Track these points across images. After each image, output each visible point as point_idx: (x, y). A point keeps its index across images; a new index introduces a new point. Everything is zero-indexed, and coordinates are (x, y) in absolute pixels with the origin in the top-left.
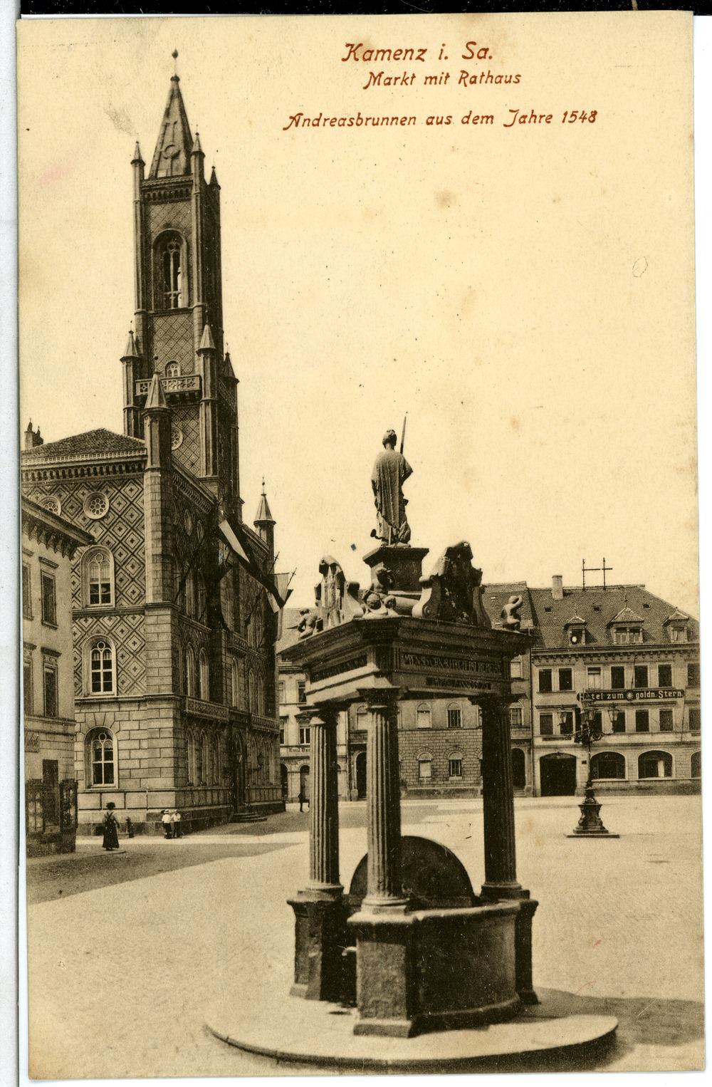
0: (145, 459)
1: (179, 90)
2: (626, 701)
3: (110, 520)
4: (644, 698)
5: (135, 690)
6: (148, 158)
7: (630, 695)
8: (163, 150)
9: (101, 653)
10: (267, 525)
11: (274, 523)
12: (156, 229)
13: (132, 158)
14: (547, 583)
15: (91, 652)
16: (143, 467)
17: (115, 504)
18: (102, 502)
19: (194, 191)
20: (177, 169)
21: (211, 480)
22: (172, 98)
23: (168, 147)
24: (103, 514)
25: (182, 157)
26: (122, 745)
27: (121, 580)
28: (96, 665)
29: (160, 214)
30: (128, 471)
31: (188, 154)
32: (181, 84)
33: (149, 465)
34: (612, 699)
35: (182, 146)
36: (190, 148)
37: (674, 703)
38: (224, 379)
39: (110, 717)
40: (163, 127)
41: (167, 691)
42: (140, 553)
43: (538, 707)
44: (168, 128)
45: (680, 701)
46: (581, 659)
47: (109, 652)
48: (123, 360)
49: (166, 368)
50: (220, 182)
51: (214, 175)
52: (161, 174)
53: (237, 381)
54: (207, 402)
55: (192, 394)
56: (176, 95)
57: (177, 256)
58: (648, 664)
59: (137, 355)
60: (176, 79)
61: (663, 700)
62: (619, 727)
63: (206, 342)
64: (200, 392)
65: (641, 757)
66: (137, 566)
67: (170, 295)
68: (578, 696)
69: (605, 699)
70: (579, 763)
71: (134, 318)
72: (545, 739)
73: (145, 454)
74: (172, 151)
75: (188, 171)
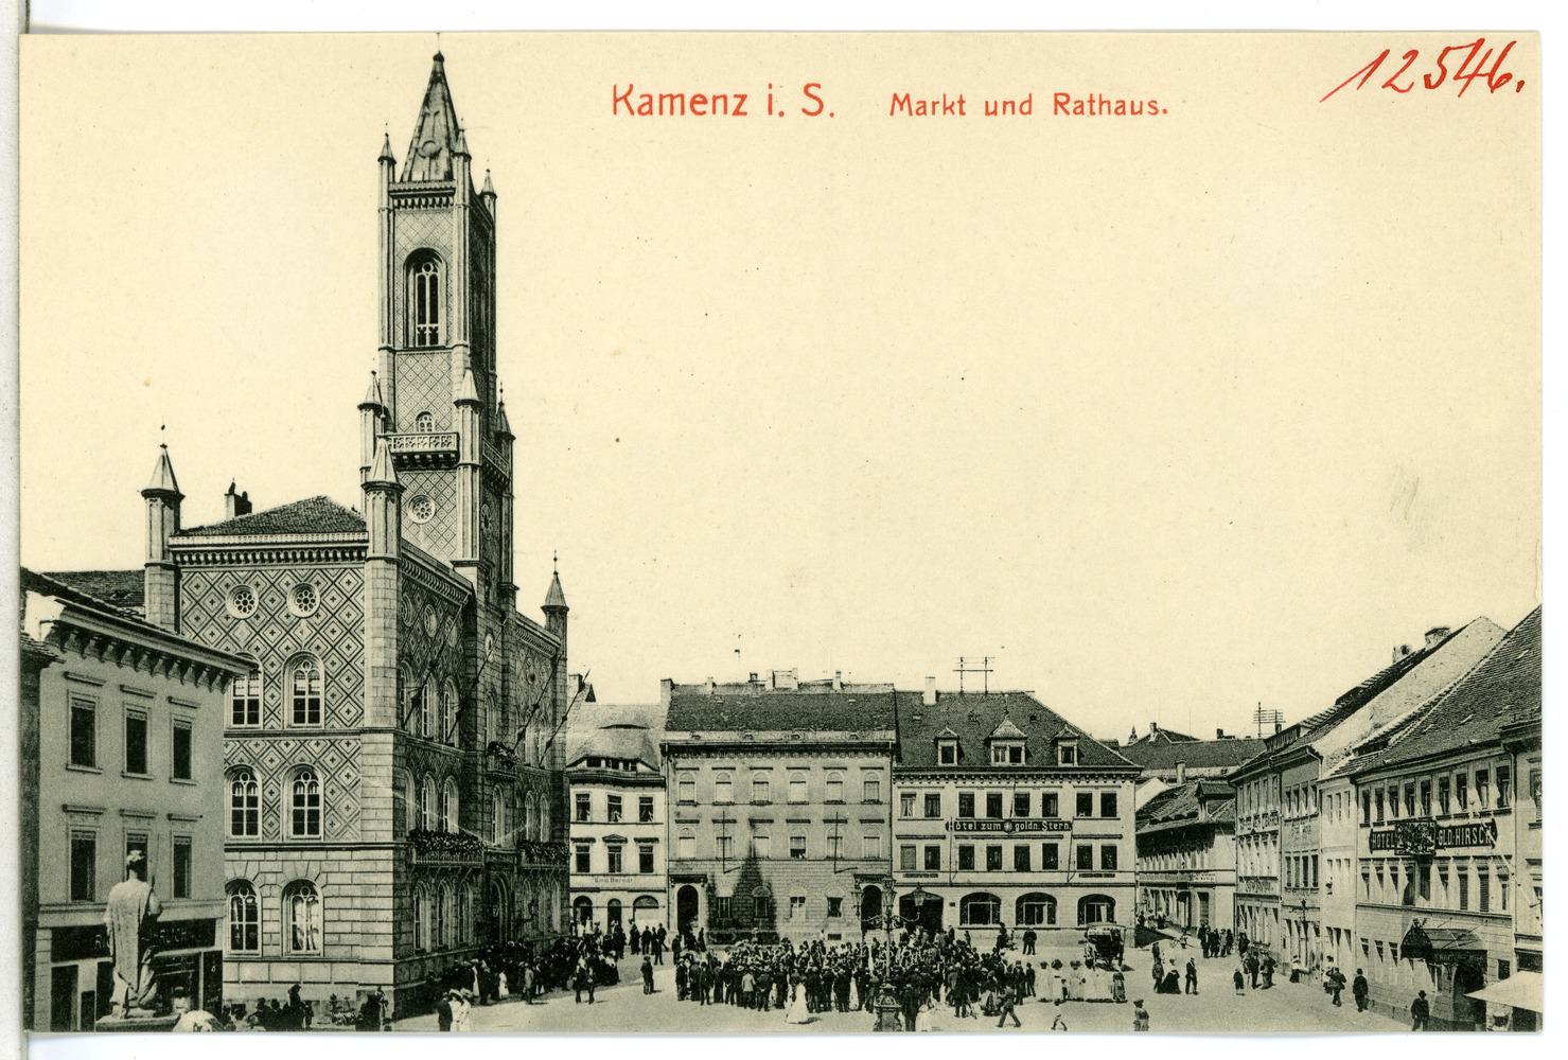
1: (443, 73)
2: (1003, 833)
3: (321, 619)
4: (1024, 830)
5: (348, 835)
6: (401, 154)
7: (1008, 826)
9: (306, 786)
10: (557, 612)
12: (407, 244)
15: (293, 783)
16: (363, 554)
17: (328, 599)
18: (311, 596)
19: (457, 199)
20: (436, 171)
21: (469, 564)
23: (426, 143)
25: (445, 154)
27: (333, 696)
28: (298, 800)
29: (414, 230)
30: (344, 558)
31: (453, 154)
32: (446, 65)
33: (370, 554)
34: (987, 830)
35: (444, 143)
37: (1061, 837)
40: (421, 118)
42: (358, 663)
43: (898, 837)
44: (427, 119)
45: (1067, 834)
46: (952, 782)
47: (317, 785)
48: (361, 407)
49: (417, 419)
51: (488, 180)
52: (417, 176)
53: (513, 438)
54: (465, 465)
55: (447, 454)
56: (438, 78)
57: (434, 279)
58: (1031, 791)
59: (378, 400)
60: (439, 58)
61: (1048, 833)
62: (994, 864)
63: (468, 390)
64: (457, 453)
65: (1020, 901)
66: (353, 680)
68: (947, 825)
69: (979, 829)
70: (946, 907)
71: (377, 354)
72: (907, 876)
73: (366, 538)
74: (430, 148)
75: (449, 176)
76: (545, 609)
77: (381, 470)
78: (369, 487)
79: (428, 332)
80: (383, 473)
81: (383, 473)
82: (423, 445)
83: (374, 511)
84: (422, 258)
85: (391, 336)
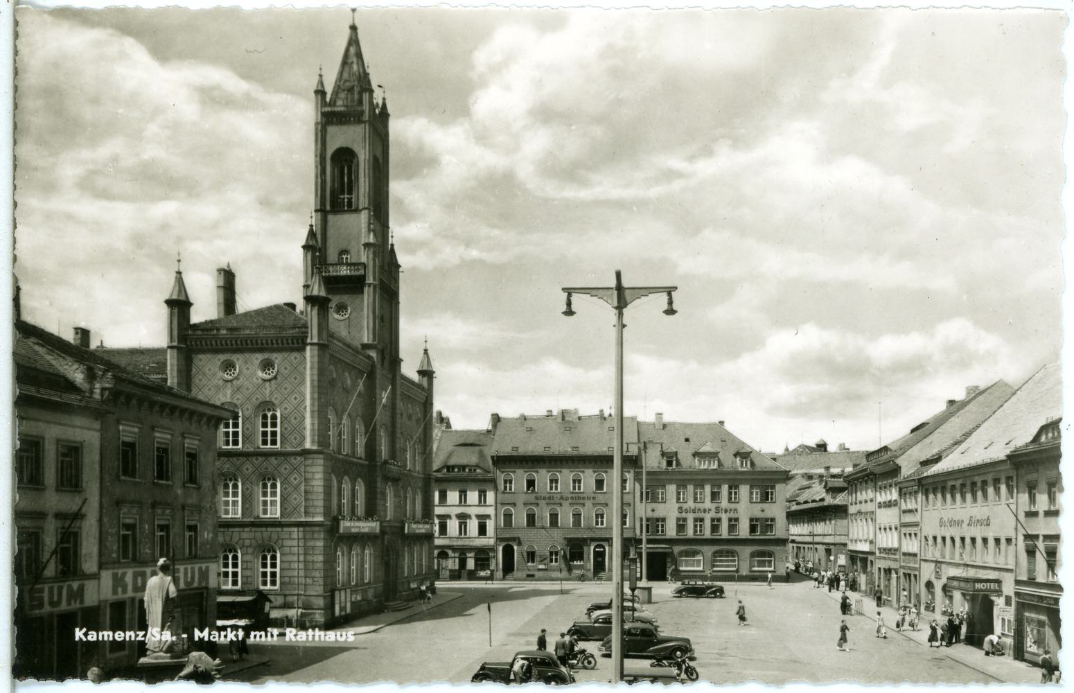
26: (285, 559)
39: (274, 537)
54: (370, 285)
71: (314, 214)
75: (360, 102)
77: (316, 287)
78: (309, 299)
79: (346, 200)
80: (317, 290)
81: (317, 290)
82: (344, 271)
83: (313, 317)
84: (344, 157)
85: (323, 203)
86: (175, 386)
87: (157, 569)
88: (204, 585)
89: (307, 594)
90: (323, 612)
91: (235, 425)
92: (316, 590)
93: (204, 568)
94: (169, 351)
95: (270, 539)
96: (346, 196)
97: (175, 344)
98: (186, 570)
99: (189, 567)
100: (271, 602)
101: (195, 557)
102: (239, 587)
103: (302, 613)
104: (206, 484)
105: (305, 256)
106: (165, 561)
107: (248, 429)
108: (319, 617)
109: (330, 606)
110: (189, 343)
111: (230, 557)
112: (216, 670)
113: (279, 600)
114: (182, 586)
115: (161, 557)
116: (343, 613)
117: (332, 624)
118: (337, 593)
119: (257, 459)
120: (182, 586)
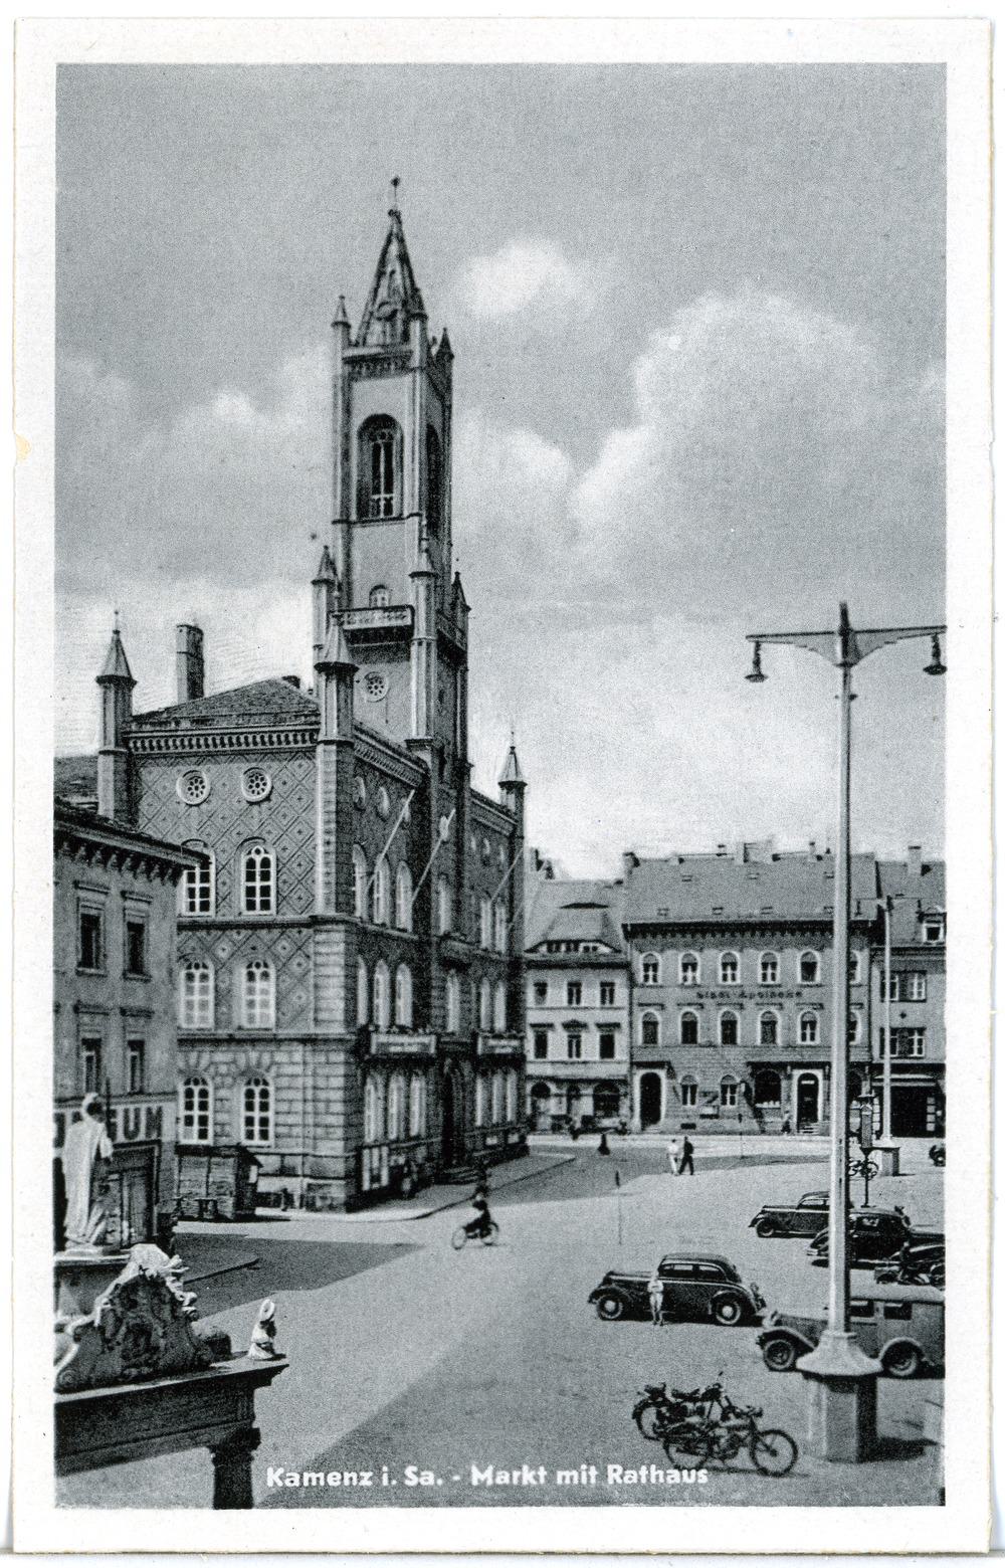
0: (316, 727)
8: (376, 306)
10: (515, 787)
11: (525, 785)
13: (331, 319)
14: (901, 855)
18: (262, 779)
22: (389, 241)
24: (263, 795)
27: (285, 882)
33: (321, 737)
36: (412, 306)
38: (450, 604)
39: (266, 1059)
41: (337, 1030)
50: (455, 348)
56: (396, 236)
67: (379, 500)
74: (387, 309)
75: (406, 337)
76: (502, 785)
78: (322, 668)
79: (382, 503)
80: (338, 654)
82: (378, 620)
83: (328, 698)
85: (345, 508)
86: (111, 815)
87: (83, 1111)
88: (154, 1137)
89: (317, 1153)
90: (343, 1182)
91: (205, 878)
92: (333, 1148)
93: (154, 1111)
94: (101, 759)
95: (259, 1064)
96: (383, 495)
97: (111, 747)
98: (126, 1111)
99: (132, 1107)
100: (260, 1165)
101: (141, 1092)
102: (209, 1141)
103: (309, 1185)
104: (157, 973)
105: (317, 597)
106: (95, 1098)
107: (224, 883)
108: (338, 1192)
109: (353, 1175)
110: (131, 745)
111: (196, 1093)
112: (174, 1274)
113: (271, 1163)
114: (121, 1138)
115: (88, 1090)
116: (376, 1186)
117: (359, 1201)
118: (366, 1152)
119: (239, 933)
120: (121, 1138)
